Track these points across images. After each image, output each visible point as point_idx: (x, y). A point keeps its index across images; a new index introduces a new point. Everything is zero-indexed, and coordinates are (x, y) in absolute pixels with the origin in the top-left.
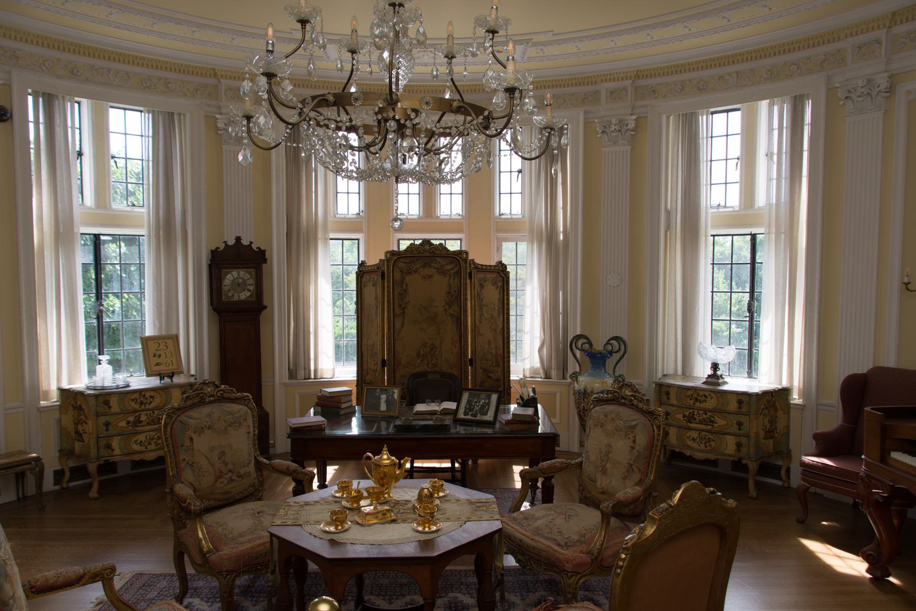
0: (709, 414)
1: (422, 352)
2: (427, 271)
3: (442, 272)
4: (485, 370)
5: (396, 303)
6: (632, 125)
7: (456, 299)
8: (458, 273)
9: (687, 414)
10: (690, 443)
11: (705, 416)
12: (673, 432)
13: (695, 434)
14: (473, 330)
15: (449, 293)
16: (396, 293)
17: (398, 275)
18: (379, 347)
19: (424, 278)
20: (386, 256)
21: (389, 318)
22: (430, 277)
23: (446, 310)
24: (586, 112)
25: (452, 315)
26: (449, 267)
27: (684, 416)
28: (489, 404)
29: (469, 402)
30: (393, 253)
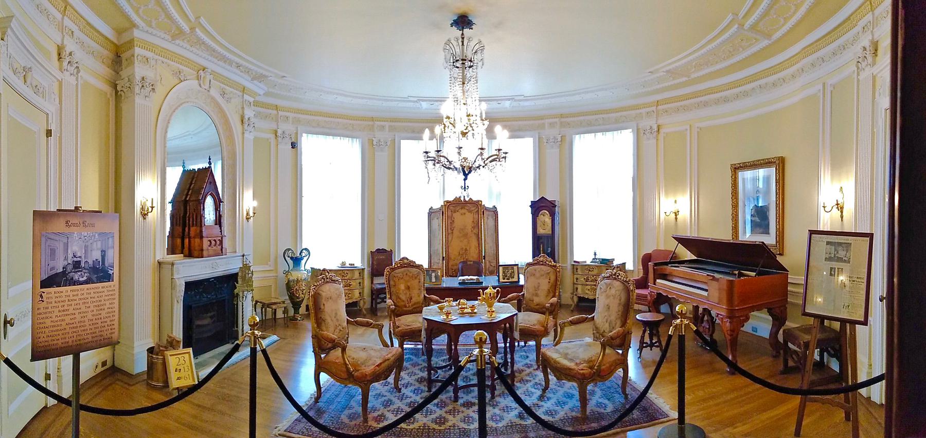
0: (595, 277)
1: (461, 253)
2: (463, 211)
3: (470, 212)
4: (489, 262)
5: (449, 227)
6: (559, 139)
7: (477, 225)
8: (478, 211)
9: (585, 278)
10: (587, 292)
11: (593, 278)
12: (580, 287)
13: (589, 287)
14: (485, 241)
15: (473, 222)
16: (449, 222)
17: (450, 213)
18: (441, 251)
19: (462, 214)
20: (444, 203)
21: (445, 235)
22: (465, 214)
23: (472, 231)
24: (539, 133)
25: (475, 233)
26: (473, 209)
27: (584, 279)
28: (513, 272)
29: (504, 272)
30: (448, 202)
